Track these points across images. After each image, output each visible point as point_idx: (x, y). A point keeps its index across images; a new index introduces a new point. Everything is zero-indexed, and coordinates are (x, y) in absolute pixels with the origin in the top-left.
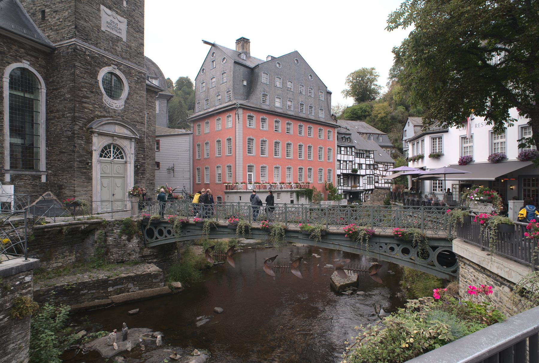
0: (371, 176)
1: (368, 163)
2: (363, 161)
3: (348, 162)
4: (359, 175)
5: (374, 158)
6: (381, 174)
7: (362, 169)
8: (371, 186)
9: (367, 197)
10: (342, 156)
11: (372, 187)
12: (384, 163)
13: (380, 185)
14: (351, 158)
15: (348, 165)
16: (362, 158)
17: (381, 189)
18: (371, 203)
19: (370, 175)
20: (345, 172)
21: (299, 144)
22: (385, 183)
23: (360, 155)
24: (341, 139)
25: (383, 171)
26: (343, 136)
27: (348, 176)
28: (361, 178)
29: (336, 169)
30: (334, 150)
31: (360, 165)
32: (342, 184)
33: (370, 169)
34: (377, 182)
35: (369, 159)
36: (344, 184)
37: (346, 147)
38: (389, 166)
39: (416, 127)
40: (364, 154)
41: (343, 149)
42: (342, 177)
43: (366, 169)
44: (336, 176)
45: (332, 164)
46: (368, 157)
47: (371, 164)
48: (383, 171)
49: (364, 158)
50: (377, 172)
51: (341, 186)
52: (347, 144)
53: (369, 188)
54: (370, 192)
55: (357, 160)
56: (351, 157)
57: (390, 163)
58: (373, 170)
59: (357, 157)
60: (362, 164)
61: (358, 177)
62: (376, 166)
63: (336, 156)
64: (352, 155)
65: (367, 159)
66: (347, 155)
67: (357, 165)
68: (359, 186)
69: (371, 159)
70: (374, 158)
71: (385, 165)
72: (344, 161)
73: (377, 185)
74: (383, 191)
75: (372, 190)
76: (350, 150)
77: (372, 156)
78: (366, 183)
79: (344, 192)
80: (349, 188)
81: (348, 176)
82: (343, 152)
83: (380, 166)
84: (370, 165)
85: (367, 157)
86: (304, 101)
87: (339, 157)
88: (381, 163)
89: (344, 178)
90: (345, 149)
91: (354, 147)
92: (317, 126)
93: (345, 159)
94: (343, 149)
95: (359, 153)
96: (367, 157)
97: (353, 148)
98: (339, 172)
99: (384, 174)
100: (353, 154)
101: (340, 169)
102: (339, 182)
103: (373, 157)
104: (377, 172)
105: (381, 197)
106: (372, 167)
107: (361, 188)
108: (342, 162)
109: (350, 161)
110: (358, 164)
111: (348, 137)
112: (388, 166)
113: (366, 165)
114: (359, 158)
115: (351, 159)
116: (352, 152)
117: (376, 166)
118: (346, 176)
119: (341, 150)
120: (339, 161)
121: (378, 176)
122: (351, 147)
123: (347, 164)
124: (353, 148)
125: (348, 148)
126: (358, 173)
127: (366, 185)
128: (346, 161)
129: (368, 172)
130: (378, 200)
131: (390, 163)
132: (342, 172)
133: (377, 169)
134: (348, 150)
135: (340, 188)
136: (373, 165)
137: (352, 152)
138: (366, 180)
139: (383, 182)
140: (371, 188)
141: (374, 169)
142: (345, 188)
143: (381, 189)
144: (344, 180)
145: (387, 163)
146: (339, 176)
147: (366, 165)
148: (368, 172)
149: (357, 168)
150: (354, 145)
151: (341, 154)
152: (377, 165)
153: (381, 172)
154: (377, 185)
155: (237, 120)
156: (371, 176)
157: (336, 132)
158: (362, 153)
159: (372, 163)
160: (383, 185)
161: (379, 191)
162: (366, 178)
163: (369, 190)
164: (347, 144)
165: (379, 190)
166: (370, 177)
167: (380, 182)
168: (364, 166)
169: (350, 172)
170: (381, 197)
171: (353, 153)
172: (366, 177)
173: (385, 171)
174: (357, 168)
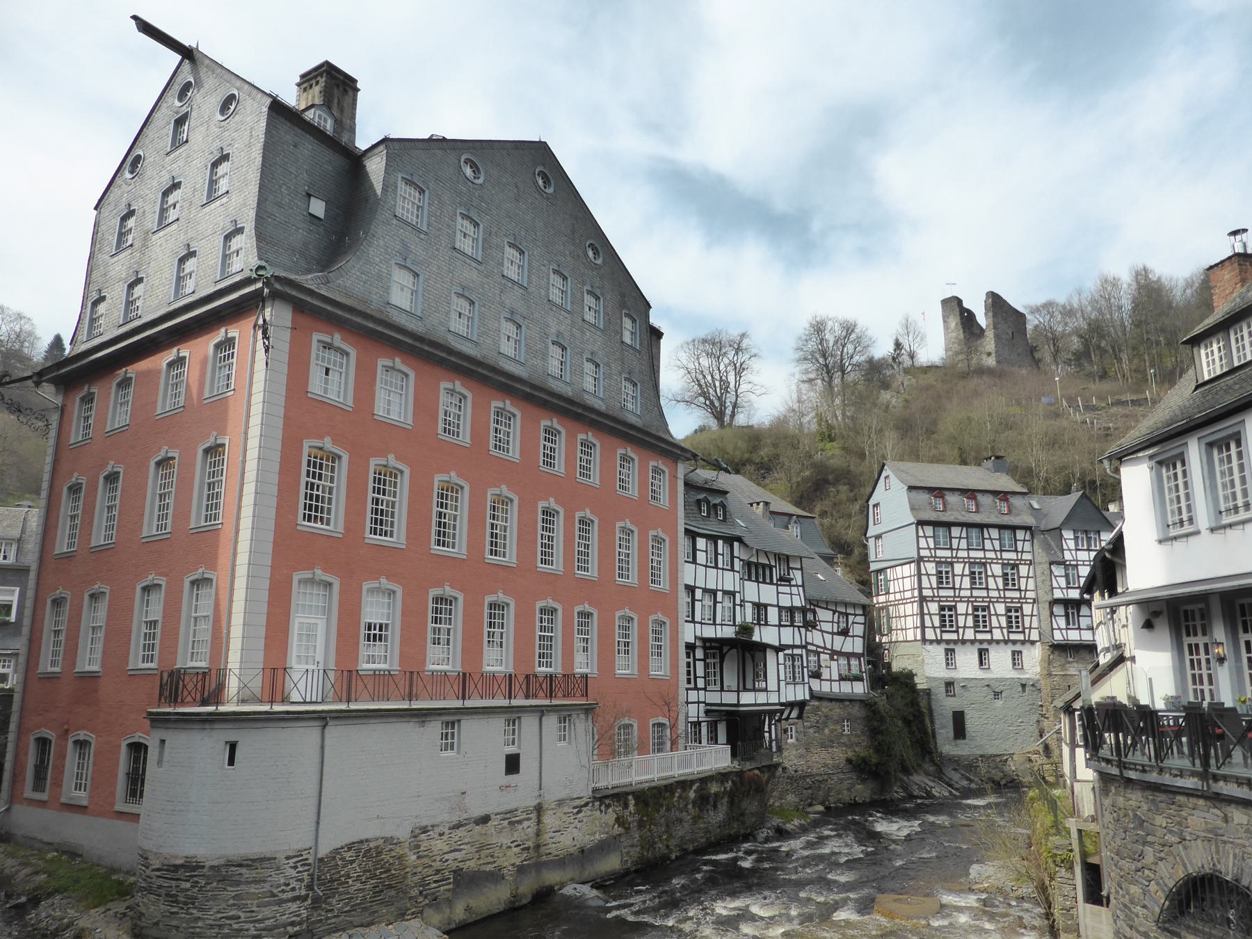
0: (797, 651)
1: (785, 601)
2: (768, 594)
3: (720, 594)
4: (763, 647)
5: (803, 586)
6: (829, 646)
7: (766, 624)
8: (799, 688)
9: (786, 731)
10: (701, 570)
11: (801, 694)
12: (836, 604)
13: (826, 687)
14: (729, 581)
15: (719, 606)
16: (764, 582)
17: (831, 700)
18: (801, 756)
19: (793, 647)
20: (709, 632)
21: (542, 505)
22: (842, 678)
23: (761, 572)
24: (695, 508)
25: (833, 634)
26: (701, 496)
27: (720, 649)
28: (770, 657)
29: (681, 621)
30: (674, 543)
31: (760, 608)
32: (701, 683)
33: (792, 625)
34: (816, 675)
35: (787, 589)
36: (707, 683)
37: (713, 539)
38: (851, 618)
39: (914, 494)
40: (771, 568)
41: (701, 543)
42: (699, 654)
43: (780, 626)
44: (682, 651)
45: (666, 602)
46: (786, 580)
47: (797, 608)
48: (833, 634)
49: (771, 583)
50: (815, 637)
51: (696, 688)
52: (713, 527)
53: (791, 698)
54: (794, 714)
55: (752, 591)
56: (729, 574)
57: (854, 606)
58: (803, 630)
59: (750, 579)
60: (766, 606)
61: (758, 655)
62: (810, 617)
63: (680, 567)
64: (732, 570)
65: (781, 589)
66: (716, 567)
67: (749, 607)
68: (766, 690)
69: (794, 590)
70: (803, 586)
71: (840, 613)
72: (705, 590)
73: (815, 685)
74: (838, 710)
75: (801, 705)
76: (727, 551)
77: (797, 576)
78: (782, 677)
79: (707, 712)
80: (730, 698)
81: (720, 649)
82: (701, 558)
83: (823, 615)
84: (791, 610)
85: (781, 579)
86: (566, 335)
87: (688, 574)
88: (827, 604)
89: (706, 656)
90: (711, 547)
91: (739, 539)
92: (615, 441)
93: (711, 586)
94: (701, 543)
95: (757, 565)
96: (781, 579)
97: (736, 544)
98: (689, 633)
99: (837, 647)
100: (737, 568)
101: (693, 621)
102: (691, 677)
103: (800, 583)
104: (815, 637)
105: (832, 731)
106: (798, 618)
107: (774, 699)
108: (698, 594)
109: (725, 593)
110: (754, 604)
111: (717, 501)
112: (847, 615)
113: (780, 608)
114: (757, 581)
115: (729, 587)
116: (732, 557)
117: (810, 617)
118: (715, 649)
119: (695, 550)
120: (691, 589)
121: (818, 654)
122: (730, 540)
123: (715, 602)
124: (736, 544)
125: (720, 542)
126: (756, 638)
127: (782, 684)
128: (714, 593)
129: (788, 636)
130: (823, 746)
131: (854, 606)
132: (698, 634)
133: (814, 627)
134: (720, 551)
135: (693, 696)
136: (803, 610)
137: (732, 557)
138: (782, 667)
139: (835, 676)
140: (800, 697)
141: (810, 625)
142: (713, 698)
143: (831, 700)
144: (706, 666)
145: (846, 605)
146: (690, 648)
147: (780, 608)
148: (788, 636)
149: (749, 619)
150: (738, 533)
151: (694, 561)
152: (815, 613)
153: (828, 637)
154: (815, 685)
155: (261, 354)
156: (797, 651)
157: (681, 475)
158: (764, 566)
159: (798, 602)
160: (836, 688)
161: (825, 707)
162: (781, 660)
163: (791, 705)
164: (713, 527)
165: (825, 704)
166: (793, 656)
167: (825, 674)
168: (773, 615)
169: (729, 632)
170: (832, 731)
171: (737, 563)
172: (781, 654)
173: (839, 633)
174: (749, 619)
